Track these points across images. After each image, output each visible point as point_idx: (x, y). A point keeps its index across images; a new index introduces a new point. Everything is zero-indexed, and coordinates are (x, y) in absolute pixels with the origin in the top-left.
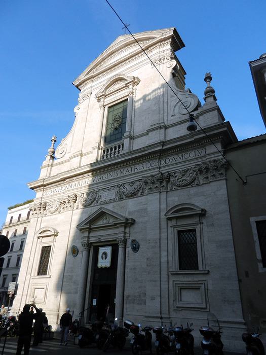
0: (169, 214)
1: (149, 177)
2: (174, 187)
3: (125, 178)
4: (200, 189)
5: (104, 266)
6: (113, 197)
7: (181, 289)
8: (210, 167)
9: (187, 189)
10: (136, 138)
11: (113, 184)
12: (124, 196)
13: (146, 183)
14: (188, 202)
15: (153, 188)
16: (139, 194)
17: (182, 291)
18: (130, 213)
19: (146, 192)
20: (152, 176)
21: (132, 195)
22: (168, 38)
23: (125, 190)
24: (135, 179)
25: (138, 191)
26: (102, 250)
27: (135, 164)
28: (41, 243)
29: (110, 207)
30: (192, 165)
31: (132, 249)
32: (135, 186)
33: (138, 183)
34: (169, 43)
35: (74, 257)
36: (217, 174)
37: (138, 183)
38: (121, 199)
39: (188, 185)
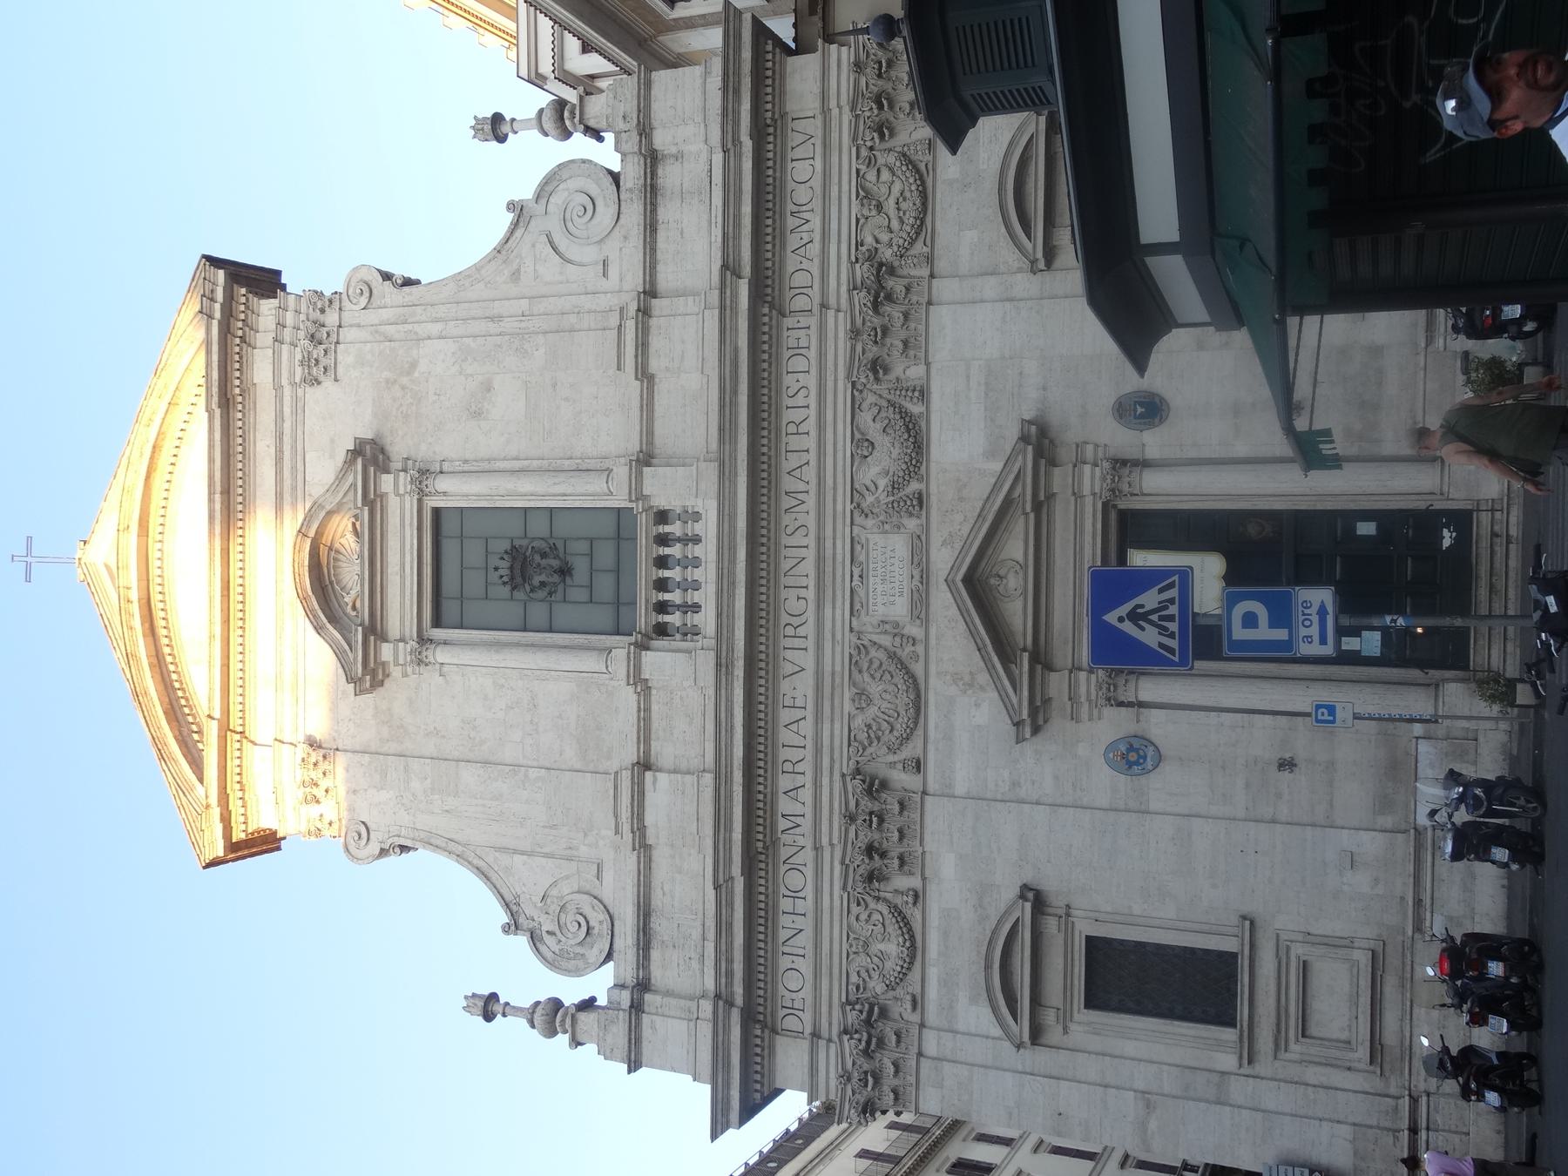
0: (1028, 245)
1: (853, 349)
2: (919, 248)
3: (829, 481)
6: (899, 545)
7: (1304, 1036)
8: (875, 89)
9: (938, 195)
10: (650, 442)
11: (843, 549)
12: (914, 486)
13: (877, 367)
14: (991, 184)
15: (903, 334)
16: (916, 409)
17: (1307, 1033)
18: (990, 454)
19: (915, 372)
20: (855, 333)
22: (230, 297)
23: (882, 483)
24: (844, 430)
25: (904, 414)
27: (778, 430)
28: (1065, 1020)
29: (944, 559)
30: (845, 162)
31: (1152, 425)
32: (874, 430)
33: (865, 418)
34: (254, 300)
35: (1159, 758)
37: (865, 418)
38: (921, 500)
39: (923, 183)
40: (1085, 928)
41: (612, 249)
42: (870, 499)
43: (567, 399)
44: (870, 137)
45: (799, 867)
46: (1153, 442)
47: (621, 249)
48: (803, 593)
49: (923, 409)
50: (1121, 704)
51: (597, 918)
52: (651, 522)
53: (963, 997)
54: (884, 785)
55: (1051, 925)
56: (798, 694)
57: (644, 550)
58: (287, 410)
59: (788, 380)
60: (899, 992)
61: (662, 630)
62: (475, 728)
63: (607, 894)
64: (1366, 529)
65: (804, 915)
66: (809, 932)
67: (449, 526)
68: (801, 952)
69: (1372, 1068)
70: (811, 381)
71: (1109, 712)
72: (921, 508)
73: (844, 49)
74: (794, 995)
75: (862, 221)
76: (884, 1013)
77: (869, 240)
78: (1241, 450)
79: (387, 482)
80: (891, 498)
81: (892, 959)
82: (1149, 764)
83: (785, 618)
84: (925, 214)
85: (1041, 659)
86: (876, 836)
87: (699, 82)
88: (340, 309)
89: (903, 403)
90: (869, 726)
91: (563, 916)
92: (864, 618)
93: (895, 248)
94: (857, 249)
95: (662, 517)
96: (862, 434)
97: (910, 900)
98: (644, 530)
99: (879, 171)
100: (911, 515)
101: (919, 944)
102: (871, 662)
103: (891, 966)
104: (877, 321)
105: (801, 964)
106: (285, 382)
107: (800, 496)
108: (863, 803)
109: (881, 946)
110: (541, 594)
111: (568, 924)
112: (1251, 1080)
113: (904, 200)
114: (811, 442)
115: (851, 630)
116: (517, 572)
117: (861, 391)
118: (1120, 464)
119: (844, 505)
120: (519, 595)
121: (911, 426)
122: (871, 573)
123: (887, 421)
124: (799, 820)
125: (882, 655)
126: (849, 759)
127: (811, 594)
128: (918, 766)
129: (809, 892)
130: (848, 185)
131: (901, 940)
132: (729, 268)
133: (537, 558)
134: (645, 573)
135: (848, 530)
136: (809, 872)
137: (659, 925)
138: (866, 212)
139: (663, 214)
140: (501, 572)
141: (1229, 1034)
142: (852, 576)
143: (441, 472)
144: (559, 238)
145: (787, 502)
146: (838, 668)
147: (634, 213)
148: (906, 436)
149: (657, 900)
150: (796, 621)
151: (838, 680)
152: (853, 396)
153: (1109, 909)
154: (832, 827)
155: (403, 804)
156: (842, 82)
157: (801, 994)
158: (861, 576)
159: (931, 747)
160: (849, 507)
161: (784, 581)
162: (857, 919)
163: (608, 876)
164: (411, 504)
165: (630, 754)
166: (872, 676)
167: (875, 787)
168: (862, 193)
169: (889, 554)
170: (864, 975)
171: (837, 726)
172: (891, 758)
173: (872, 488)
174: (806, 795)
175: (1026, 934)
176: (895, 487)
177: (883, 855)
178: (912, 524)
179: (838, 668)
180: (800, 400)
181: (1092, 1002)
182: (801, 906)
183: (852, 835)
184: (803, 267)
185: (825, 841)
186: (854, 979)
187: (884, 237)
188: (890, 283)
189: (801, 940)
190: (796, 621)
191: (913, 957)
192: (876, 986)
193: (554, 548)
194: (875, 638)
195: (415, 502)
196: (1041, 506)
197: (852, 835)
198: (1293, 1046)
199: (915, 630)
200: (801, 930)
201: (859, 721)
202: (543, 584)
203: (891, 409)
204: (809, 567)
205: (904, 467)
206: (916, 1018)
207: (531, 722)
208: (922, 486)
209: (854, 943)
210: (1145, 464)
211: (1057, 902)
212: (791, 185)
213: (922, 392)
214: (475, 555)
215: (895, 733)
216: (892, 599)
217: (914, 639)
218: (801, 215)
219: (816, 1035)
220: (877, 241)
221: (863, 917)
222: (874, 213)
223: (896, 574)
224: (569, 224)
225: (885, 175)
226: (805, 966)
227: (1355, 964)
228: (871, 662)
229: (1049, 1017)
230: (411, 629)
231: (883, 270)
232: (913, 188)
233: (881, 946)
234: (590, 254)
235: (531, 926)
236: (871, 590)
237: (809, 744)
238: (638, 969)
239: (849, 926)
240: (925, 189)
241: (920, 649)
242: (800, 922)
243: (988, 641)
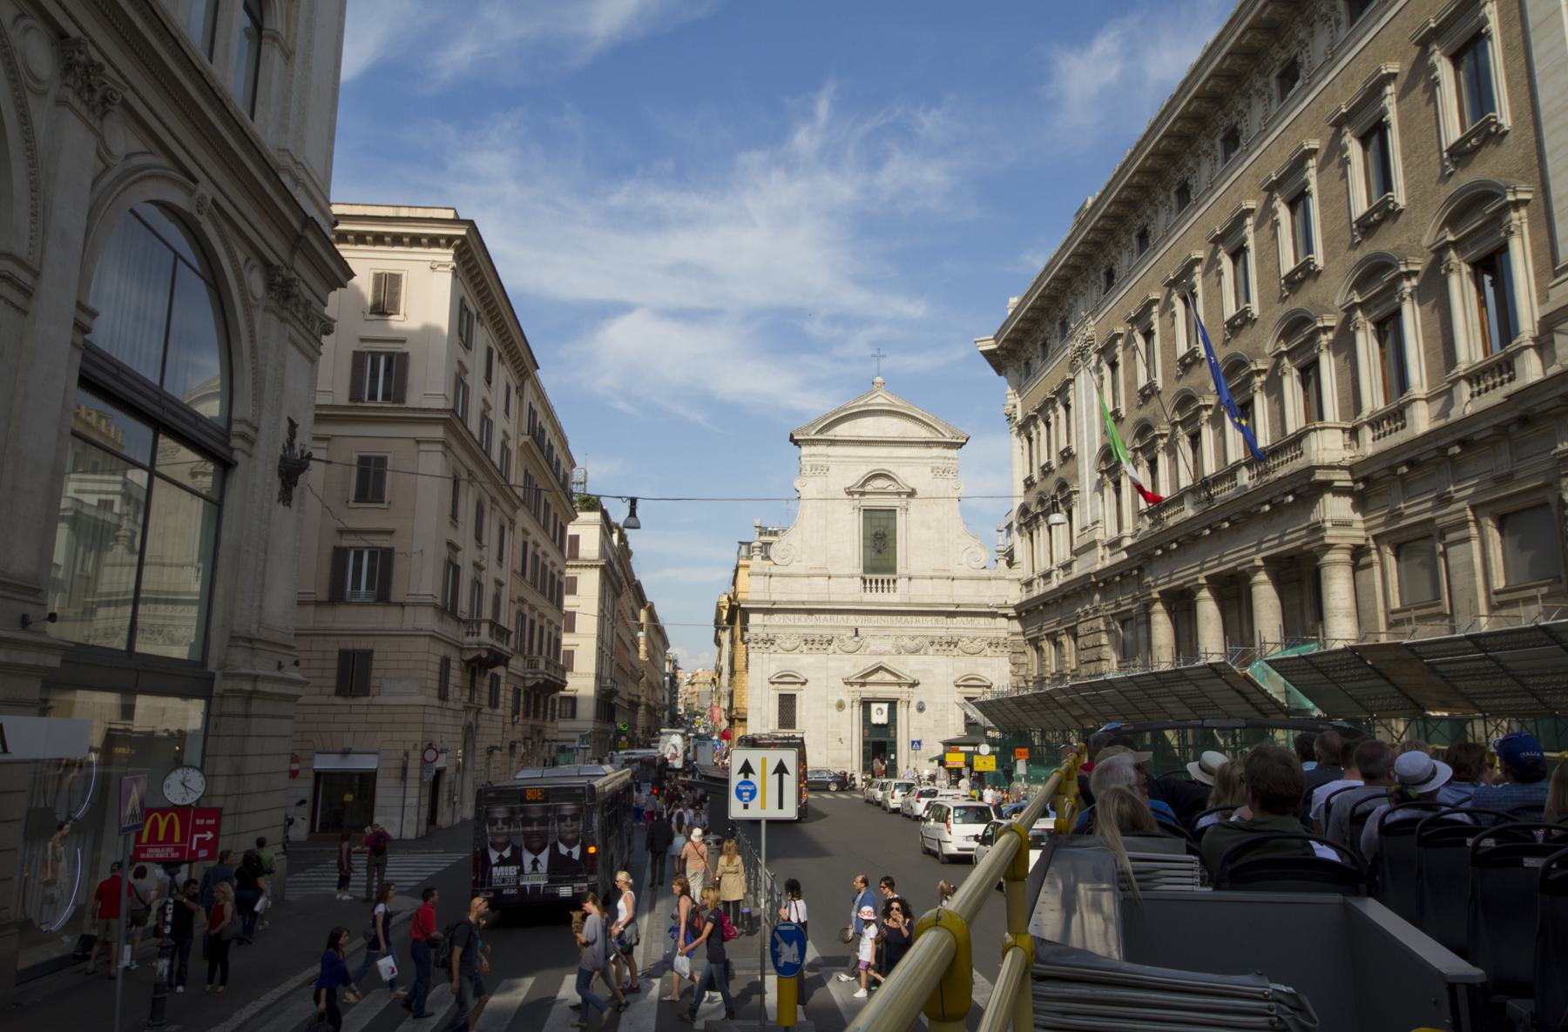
2: (961, 652)
4: (987, 660)
5: (880, 722)
6: (889, 648)
11: (887, 633)
13: (932, 643)
16: (922, 652)
18: (911, 671)
21: (915, 652)
24: (918, 633)
26: (874, 707)
29: (886, 661)
32: (916, 641)
44: (989, 641)
46: (913, 709)
55: (799, 686)
57: (886, 577)
61: (865, 582)
63: (794, 564)
64: (893, 757)
66: (790, 623)
67: (891, 514)
70: (929, 625)
71: (850, 700)
78: (911, 730)
85: (863, 684)
95: (894, 581)
98: (891, 577)
103: (784, 645)
114: (914, 625)
118: (909, 702)
119: (898, 633)
127: (876, 624)
129: (800, 624)
130: (977, 634)
132: (958, 606)
134: (880, 577)
144: (968, 551)
147: (974, 573)
154: (819, 631)
165: (832, 572)
167: (830, 642)
175: (796, 680)
181: (780, 695)
188: (953, 646)
192: (778, 641)
196: (899, 685)
204: (883, 624)
210: (908, 706)
211: (803, 687)
214: (884, 523)
226: (781, 622)
229: (776, 685)
230: (863, 503)
234: (964, 560)
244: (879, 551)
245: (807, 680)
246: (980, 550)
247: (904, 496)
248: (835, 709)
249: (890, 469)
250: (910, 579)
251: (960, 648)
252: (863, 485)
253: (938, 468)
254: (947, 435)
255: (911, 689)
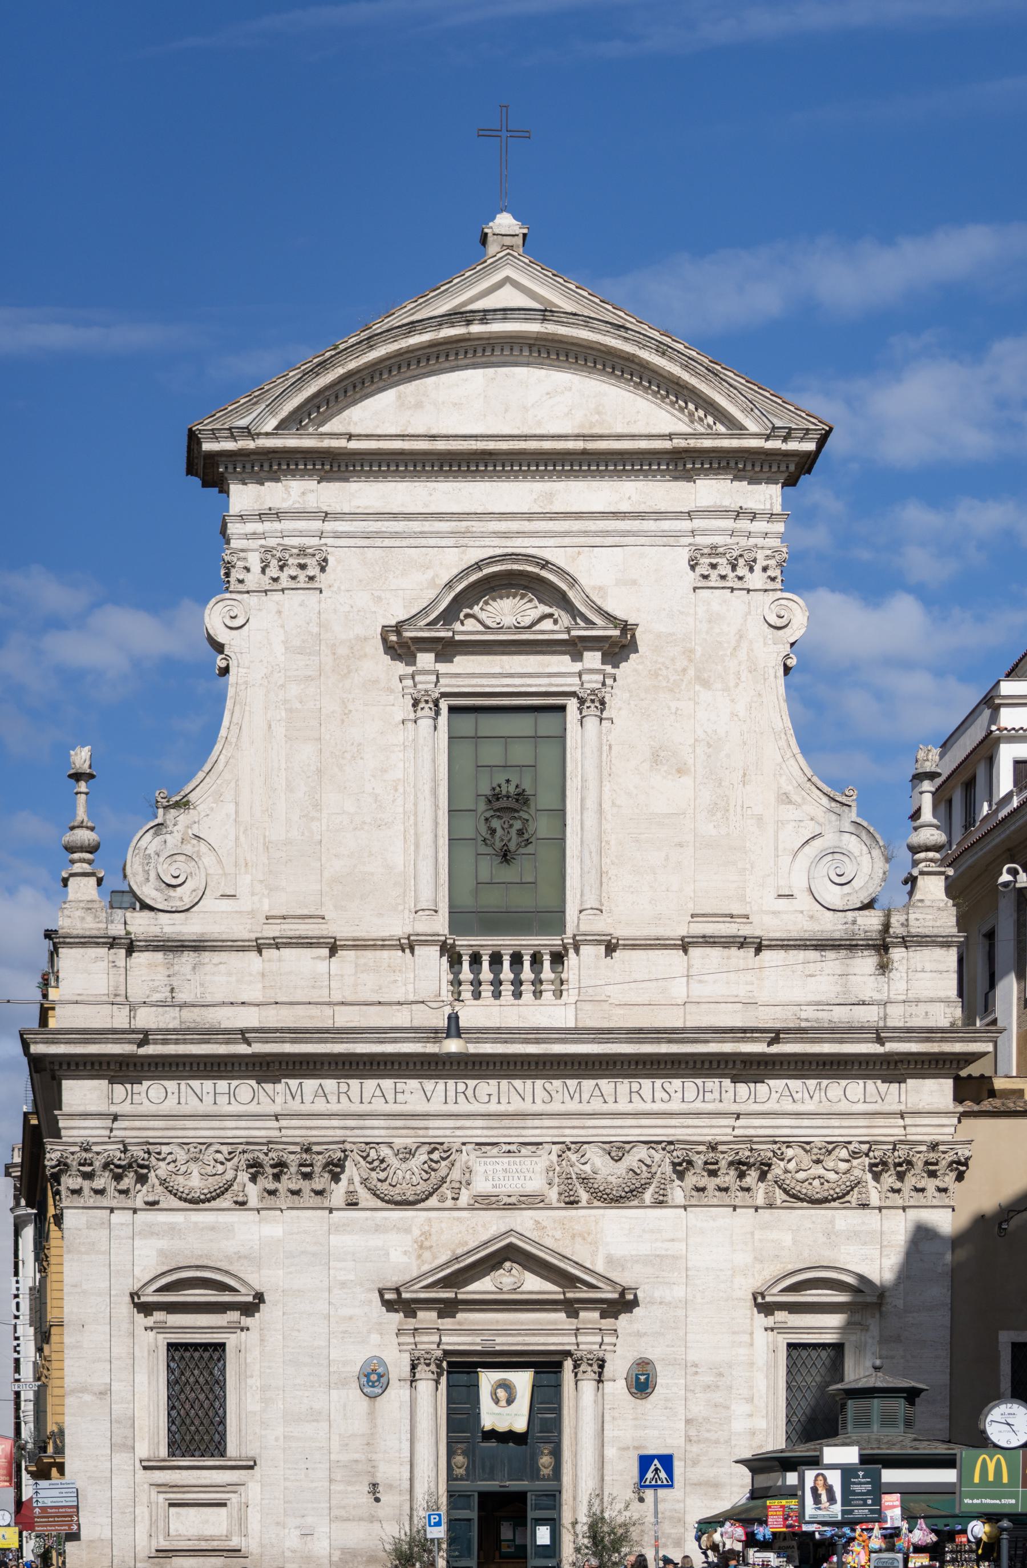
2: (779, 1196)
11: (531, 1135)
12: (584, 1196)
16: (648, 1196)
19: (677, 1194)
23: (587, 1168)
24: (634, 1134)
28: (159, 1328)
32: (631, 1160)
33: (642, 1152)
36: (931, 1184)
40: (231, 1341)
41: (804, 901)
42: (574, 1157)
43: (667, 858)
45: (256, 1099)
46: (617, 1388)
47: (802, 912)
48: (494, 1099)
49: (648, 1202)
50: (414, 1367)
51: (184, 895)
52: (554, 949)
53: (162, 1243)
54: (336, 1178)
55: (234, 1316)
56: (407, 1096)
58: (666, 525)
59: (677, 1083)
60: (160, 1189)
62: (354, 758)
65: (215, 1103)
66: (201, 1108)
68: (183, 1101)
69: (153, 1551)
72: (567, 1203)
73: (952, 1130)
74: (144, 1095)
75: (808, 1147)
76: (142, 1179)
77: (789, 1153)
78: (610, 1452)
79: (593, 659)
80: (574, 1176)
81: (186, 1183)
82: (367, 1390)
83: (471, 1083)
84: (808, 1202)
85: (448, 1308)
86: (293, 1169)
87: (942, 994)
88: (766, 591)
89: (653, 1185)
90: (382, 1161)
91: (182, 858)
92: (472, 1156)
93: (782, 1177)
94: (784, 1142)
95: (558, 959)
96: (628, 1152)
97: (240, 1199)
99: (848, 1161)
100: (560, 1194)
101: (201, 1206)
102: (436, 1162)
103: (179, 1182)
104: (723, 1164)
105: (172, 1100)
106: (697, 523)
107: (577, 1095)
108: (320, 1157)
109: (195, 1173)
110: (483, 829)
111: (175, 865)
112: (132, 1468)
113: (822, 1184)
114: (623, 1106)
115: (464, 1144)
116: (503, 803)
117: (664, 1149)
118: (602, 1364)
119: (570, 1135)
120: (482, 806)
121: (635, 1193)
122: (512, 1159)
123: (638, 1172)
124: (298, 1098)
125: (443, 1172)
126: (354, 1143)
128: (352, 1204)
129: (235, 1108)
131: (206, 1191)
133: (518, 825)
135: (549, 1139)
136: (253, 1108)
137: (188, 958)
138: (815, 1151)
139: (831, 955)
140: (504, 786)
141: (163, 1452)
142: (509, 1143)
143: (601, 719)
145: (572, 1083)
146: (431, 1132)
147: (832, 926)
148: (627, 1189)
149: (206, 956)
150: (469, 1093)
151: (421, 1132)
152: (660, 1142)
153: (248, 1361)
155: (272, 672)
156: (923, 1131)
157: (145, 1101)
158: (509, 1152)
159: (368, 1213)
160: (568, 1140)
161: (504, 1083)
162: (218, 1152)
163: (226, 905)
164: (571, 684)
166: (425, 1162)
168: (830, 1147)
169: (528, 1175)
170: (169, 1158)
171: (383, 1132)
172: (357, 1180)
173: (583, 1160)
174: (320, 1106)
175: (226, 1298)
176: (584, 1180)
177: (277, 1177)
178: (553, 1195)
179: (431, 1132)
180: (660, 1094)
181: (172, 1347)
182: (223, 1100)
183: (292, 1148)
184: (773, 1093)
185: (283, 1123)
186: (165, 1149)
187: (792, 1166)
189: (194, 1101)
190: (469, 1093)
191: (191, 1201)
192: (163, 1169)
193: (528, 842)
194: (457, 1165)
195: (572, 689)
197: (292, 1148)
198: (162, 1496)
199: (464, 1199)
200: (201, 1100)
201: (385, 1151)
202: (493, 831)
203: (649, 1175)
205: (601, 1188)
206: (139, 1203)
207: (364, 823)
208: (584, 1203)
209: (197, 1150)
212: (844, 1082)
213: (661, 1202)
215: (379, 1184)
216: (490, 1178)
217: (457, 1199)
218: (817, 1091)
219: (115, 1118)
220: (789, 1161)
221: (219, 1156)
222: (814, 1158)
223: (511, 1182)
224: (830, 857)
225: (843, 1166)
226: (170, 1105)
227: (228, 1538)
228: (436, 1162)
229: (159, 1316)
230: (447, 685)
231: (764, 1169)
232: (832, 1192)
233: (195, 1173)
234: (798, 883)
235: (168, 822)
236: (497, 1160)
237: (365, 1108)
238: (146, 941)
239: (210, 1144)
240: (829, 1201)
241: (450, 1203)
242: (208, 1099)
243: (462, 1265)
244: (506, 856)
245: (260, 1297)
246: (852, 844)
247: (593, 659)
248: (354, 1393)
249: (547, 554)
250: (611, 949)
251: (778, 1183)
252: (449, 616)
253: (714, 551)
254: (752, 427)
255: (607, 1323)
